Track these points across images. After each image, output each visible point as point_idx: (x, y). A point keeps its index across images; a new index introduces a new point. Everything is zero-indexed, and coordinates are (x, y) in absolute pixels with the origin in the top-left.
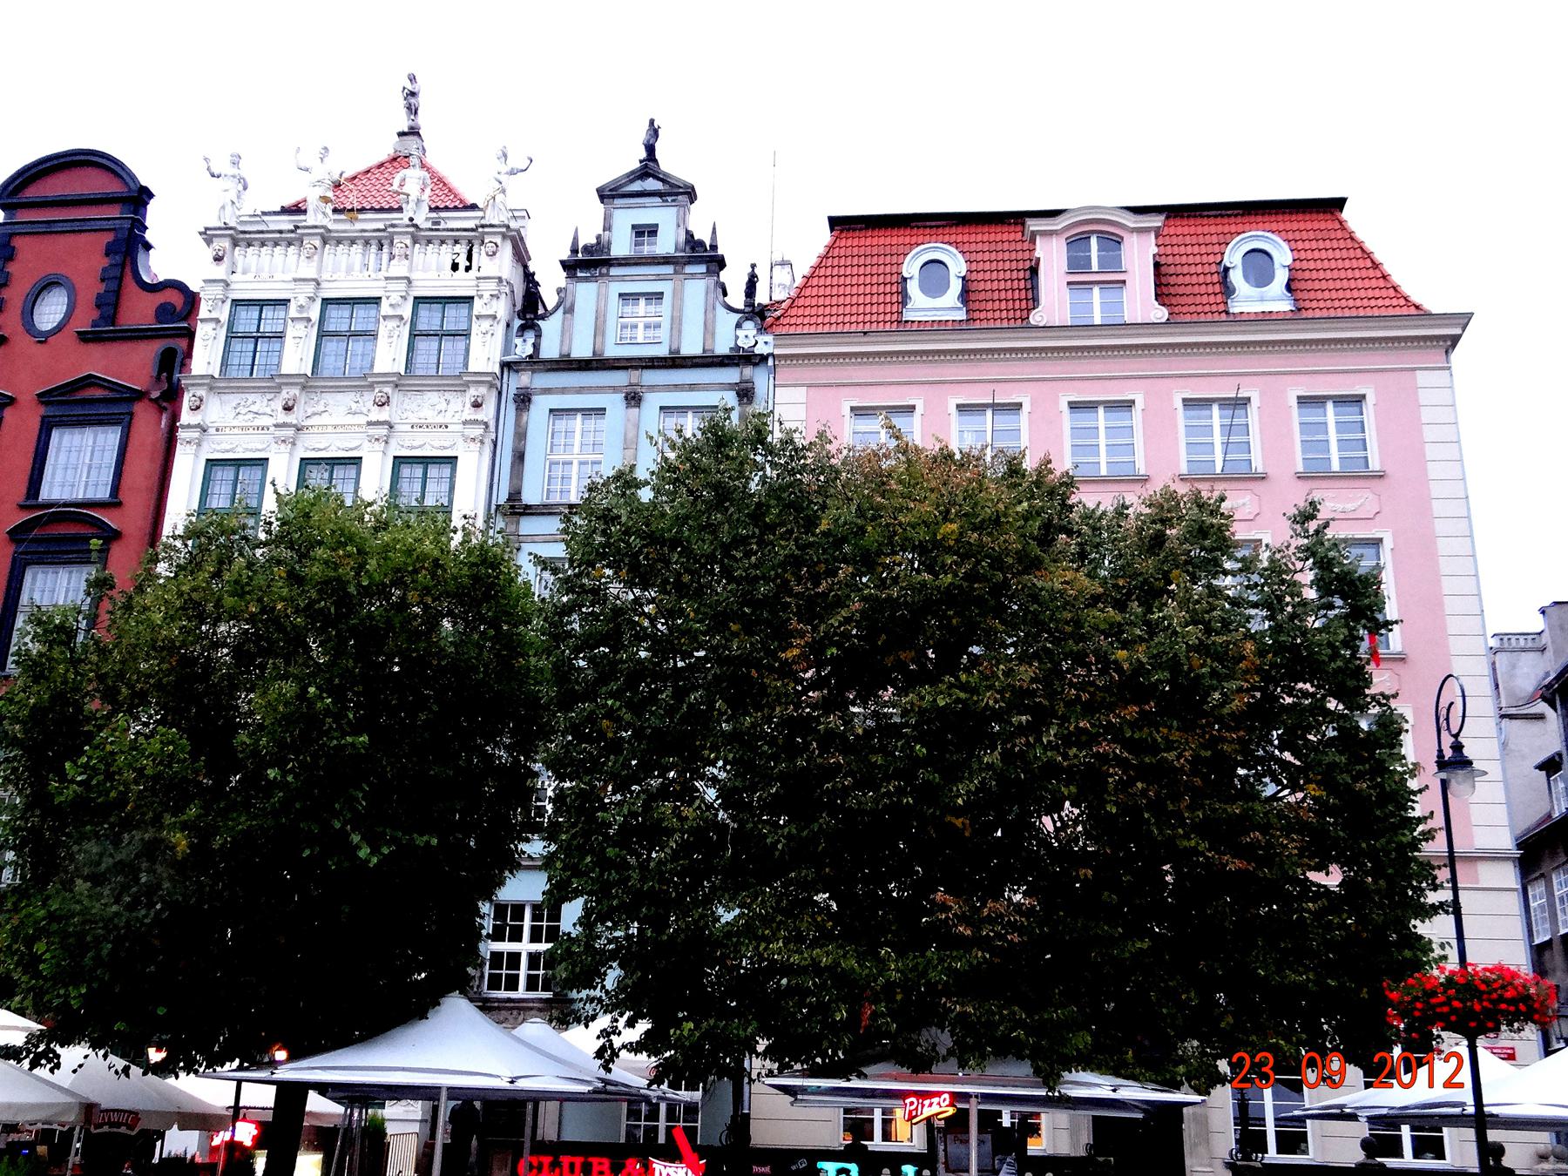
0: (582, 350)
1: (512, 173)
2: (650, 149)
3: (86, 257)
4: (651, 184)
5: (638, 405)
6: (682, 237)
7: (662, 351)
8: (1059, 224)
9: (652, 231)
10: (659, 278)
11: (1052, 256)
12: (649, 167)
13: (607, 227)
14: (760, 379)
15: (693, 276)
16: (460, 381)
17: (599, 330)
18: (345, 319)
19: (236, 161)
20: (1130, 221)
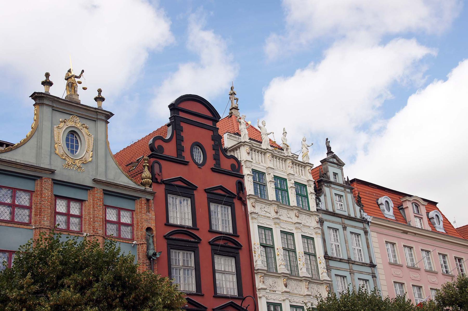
0: (331, 210)
4: (335, 161)
5: (346, 230)
7: (346, 214)
10: (342, 191)
17: (333, 205)
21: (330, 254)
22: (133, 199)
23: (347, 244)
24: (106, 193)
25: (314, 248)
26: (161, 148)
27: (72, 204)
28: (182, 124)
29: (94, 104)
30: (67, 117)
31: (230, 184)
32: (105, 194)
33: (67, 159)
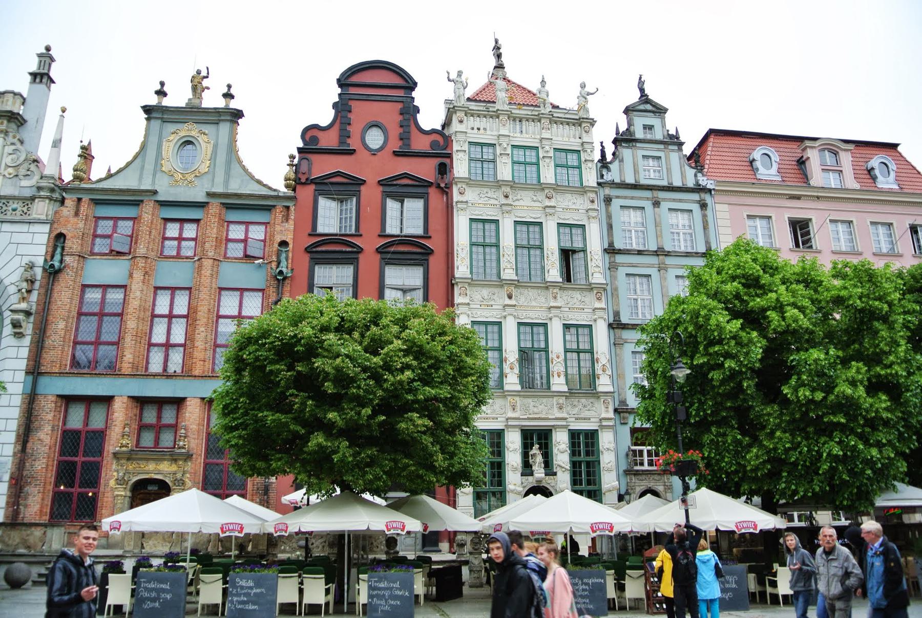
0: (630, 180)
1: (589, 94)
2: (642, 90)
3: (389, 113)
6: (666, 133)
8: (817, 143)
9: (650, 127)
10: (659, 150)
11: (814, 158)
12: (644, 98)
13: (630, 123)
14: (708, 198)
15: (673, 150)
16: (582, 190)
17: (636, 172)
18: (527, 158)
19: (460, 74)
20: (844, 146)
21: (618, 245)
22: (269, 209)
23: (658, 228)
24: (229, 207)
25: (585, 239)
26: (315, 140)
27: (187, 226)
28: (350, 103)
29: (221, 103)
30: (179, 126)
31: (425, 169)
32: (227, 208)
33: (175, 175)
